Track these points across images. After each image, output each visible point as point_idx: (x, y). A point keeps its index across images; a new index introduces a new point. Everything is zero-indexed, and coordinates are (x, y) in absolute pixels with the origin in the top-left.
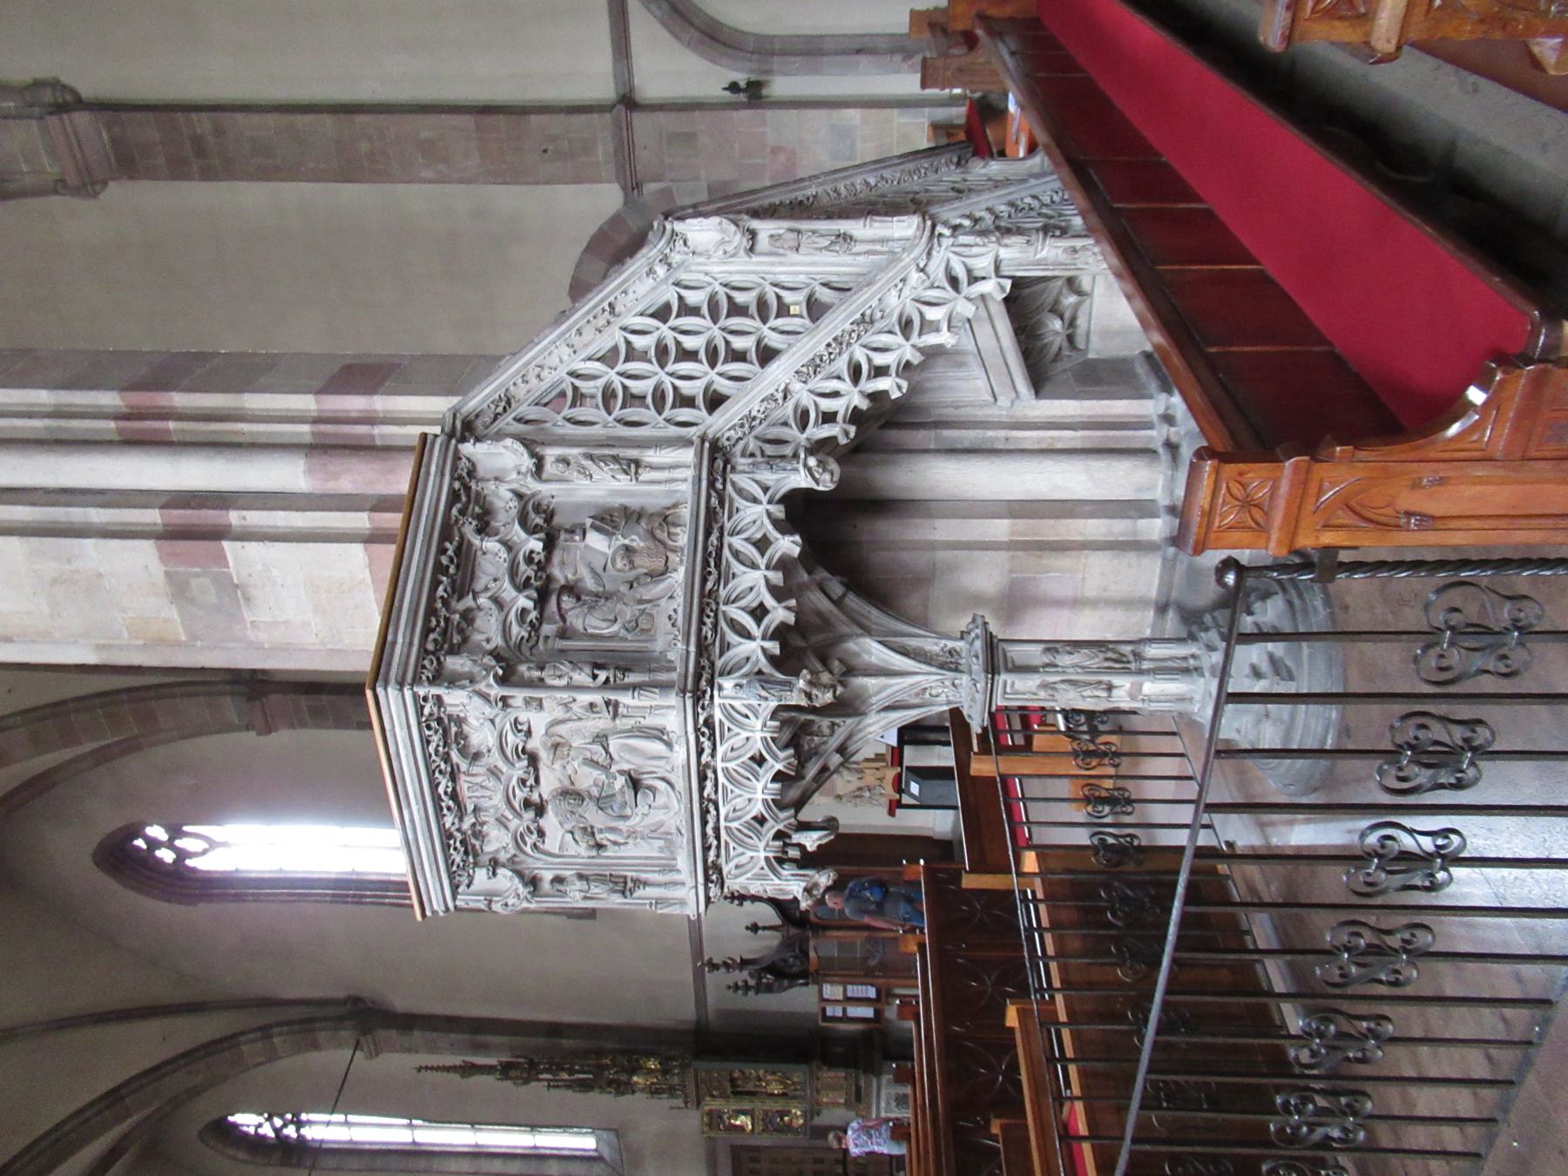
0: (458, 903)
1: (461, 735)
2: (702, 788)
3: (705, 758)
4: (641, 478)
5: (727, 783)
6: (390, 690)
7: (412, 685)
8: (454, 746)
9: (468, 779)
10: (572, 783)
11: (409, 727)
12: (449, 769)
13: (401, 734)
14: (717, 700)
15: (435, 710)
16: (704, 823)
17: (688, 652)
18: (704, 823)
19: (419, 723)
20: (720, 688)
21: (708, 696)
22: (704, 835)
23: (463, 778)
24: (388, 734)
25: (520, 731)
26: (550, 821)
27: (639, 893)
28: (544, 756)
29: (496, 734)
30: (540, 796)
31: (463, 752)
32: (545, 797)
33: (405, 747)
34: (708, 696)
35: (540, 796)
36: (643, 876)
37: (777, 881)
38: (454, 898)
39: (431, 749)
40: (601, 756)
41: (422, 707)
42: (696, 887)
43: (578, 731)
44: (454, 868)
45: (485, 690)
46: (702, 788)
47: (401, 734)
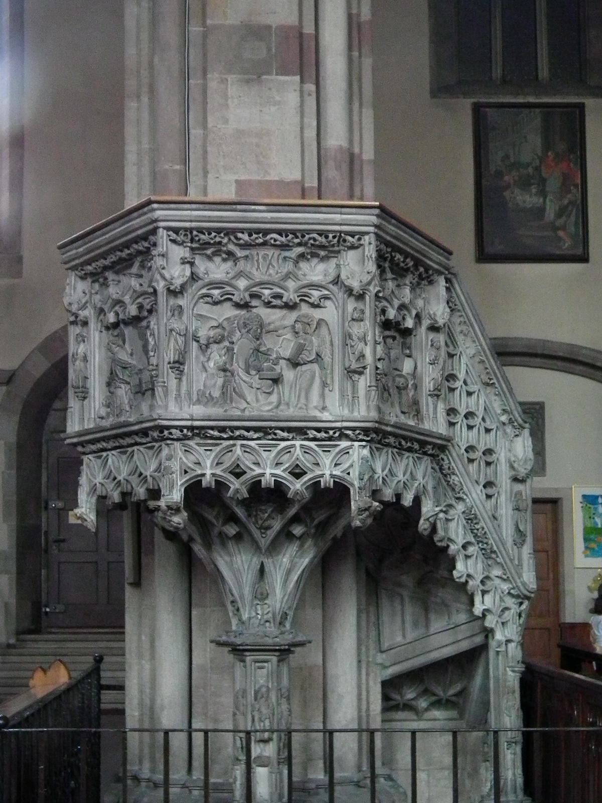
0: (161, 230)
1: (314, 255)
2: (282, 429)
3: (312, 434)
4: (429, 398)
5: (279, 448)
6: (375, 217)
7: (376, 234)
8: (309, 251)
9: (276, 255)
10: (268, 332)
11: (341, 225)
12: (291, 244)
13: (338, 217)
14: (356, 444)
15: (349, 244)
16: (248, 429)
17: (387, 425)
18: (248, 429)
19: (341, 232)
20: (364, 447)
21: (365, 438)
22: (238, 428)
23: (277, 252)
24: (339, 210)
25: (320, 300)
26: (228, 312)
27: (173, 375)
28: (293, 316)
29: (323, 283)
30: (256, 307)
31: (302, 256)
32: (254, 310)
33: (325, 219)
34: (365, 438)
35: (256, 307)
36: (184, 378)
37: (179, 483)
38: (164, 228)
39: (315, 235)
40: (304, 357)
41: (353, 236)
42: (192, 420)
43: (323, 341)
44: (195, 233)
45: (373, 283)
46: (282, 429)
47: (338, 217)
